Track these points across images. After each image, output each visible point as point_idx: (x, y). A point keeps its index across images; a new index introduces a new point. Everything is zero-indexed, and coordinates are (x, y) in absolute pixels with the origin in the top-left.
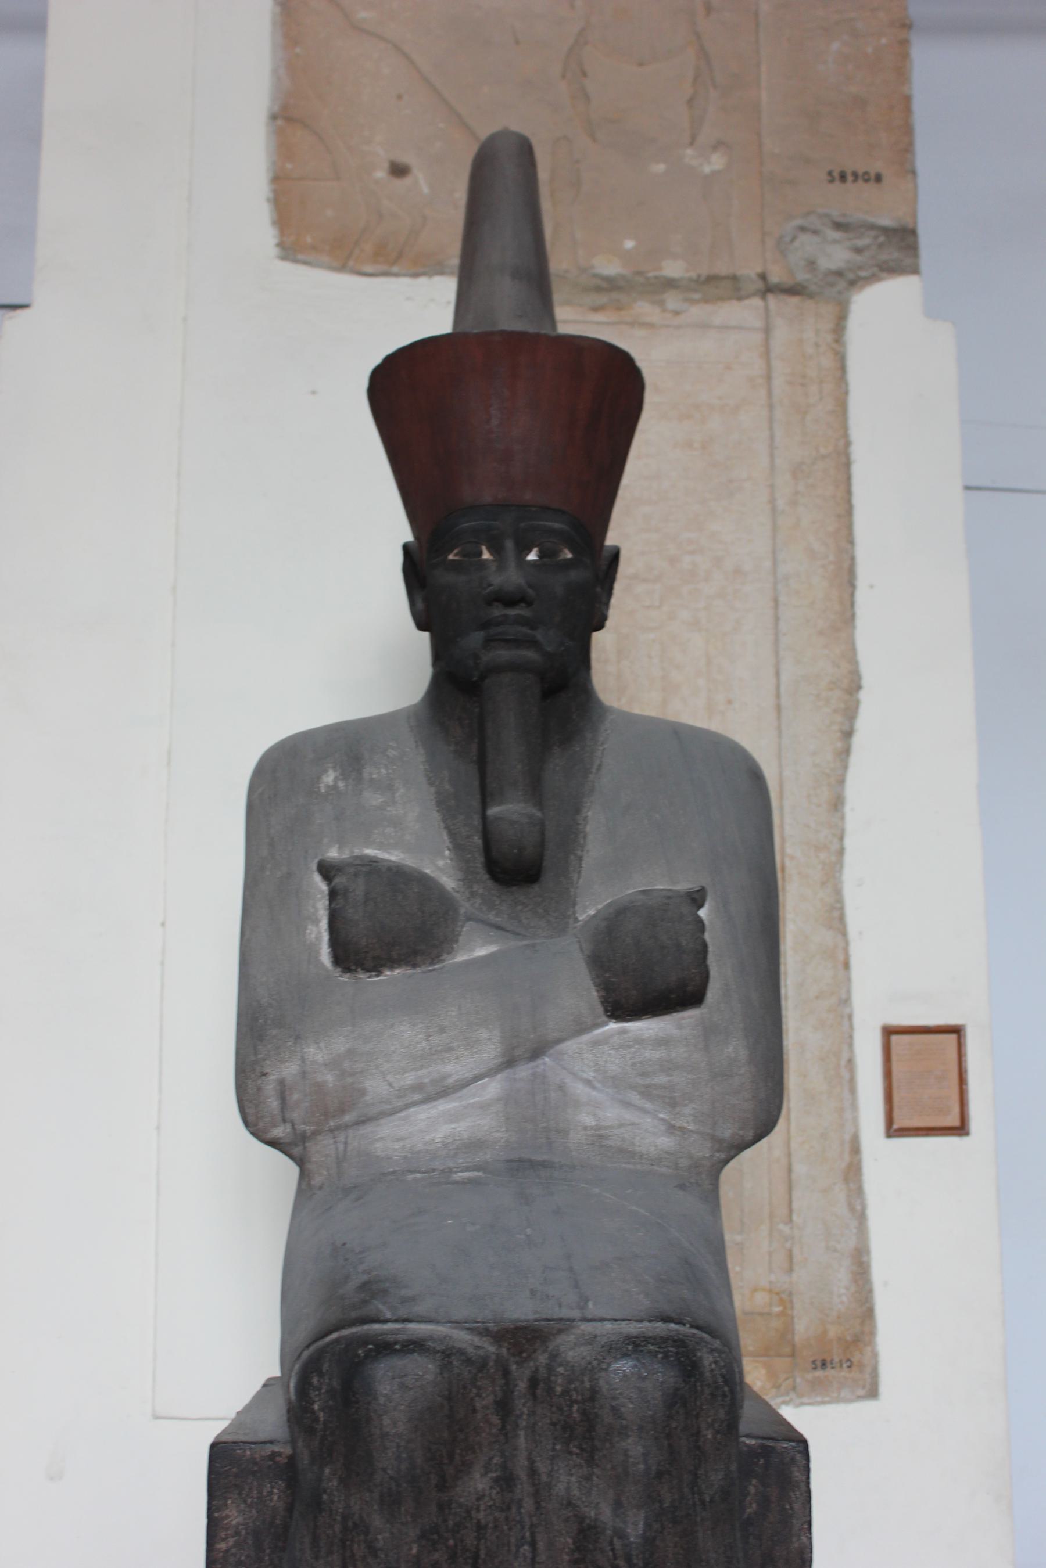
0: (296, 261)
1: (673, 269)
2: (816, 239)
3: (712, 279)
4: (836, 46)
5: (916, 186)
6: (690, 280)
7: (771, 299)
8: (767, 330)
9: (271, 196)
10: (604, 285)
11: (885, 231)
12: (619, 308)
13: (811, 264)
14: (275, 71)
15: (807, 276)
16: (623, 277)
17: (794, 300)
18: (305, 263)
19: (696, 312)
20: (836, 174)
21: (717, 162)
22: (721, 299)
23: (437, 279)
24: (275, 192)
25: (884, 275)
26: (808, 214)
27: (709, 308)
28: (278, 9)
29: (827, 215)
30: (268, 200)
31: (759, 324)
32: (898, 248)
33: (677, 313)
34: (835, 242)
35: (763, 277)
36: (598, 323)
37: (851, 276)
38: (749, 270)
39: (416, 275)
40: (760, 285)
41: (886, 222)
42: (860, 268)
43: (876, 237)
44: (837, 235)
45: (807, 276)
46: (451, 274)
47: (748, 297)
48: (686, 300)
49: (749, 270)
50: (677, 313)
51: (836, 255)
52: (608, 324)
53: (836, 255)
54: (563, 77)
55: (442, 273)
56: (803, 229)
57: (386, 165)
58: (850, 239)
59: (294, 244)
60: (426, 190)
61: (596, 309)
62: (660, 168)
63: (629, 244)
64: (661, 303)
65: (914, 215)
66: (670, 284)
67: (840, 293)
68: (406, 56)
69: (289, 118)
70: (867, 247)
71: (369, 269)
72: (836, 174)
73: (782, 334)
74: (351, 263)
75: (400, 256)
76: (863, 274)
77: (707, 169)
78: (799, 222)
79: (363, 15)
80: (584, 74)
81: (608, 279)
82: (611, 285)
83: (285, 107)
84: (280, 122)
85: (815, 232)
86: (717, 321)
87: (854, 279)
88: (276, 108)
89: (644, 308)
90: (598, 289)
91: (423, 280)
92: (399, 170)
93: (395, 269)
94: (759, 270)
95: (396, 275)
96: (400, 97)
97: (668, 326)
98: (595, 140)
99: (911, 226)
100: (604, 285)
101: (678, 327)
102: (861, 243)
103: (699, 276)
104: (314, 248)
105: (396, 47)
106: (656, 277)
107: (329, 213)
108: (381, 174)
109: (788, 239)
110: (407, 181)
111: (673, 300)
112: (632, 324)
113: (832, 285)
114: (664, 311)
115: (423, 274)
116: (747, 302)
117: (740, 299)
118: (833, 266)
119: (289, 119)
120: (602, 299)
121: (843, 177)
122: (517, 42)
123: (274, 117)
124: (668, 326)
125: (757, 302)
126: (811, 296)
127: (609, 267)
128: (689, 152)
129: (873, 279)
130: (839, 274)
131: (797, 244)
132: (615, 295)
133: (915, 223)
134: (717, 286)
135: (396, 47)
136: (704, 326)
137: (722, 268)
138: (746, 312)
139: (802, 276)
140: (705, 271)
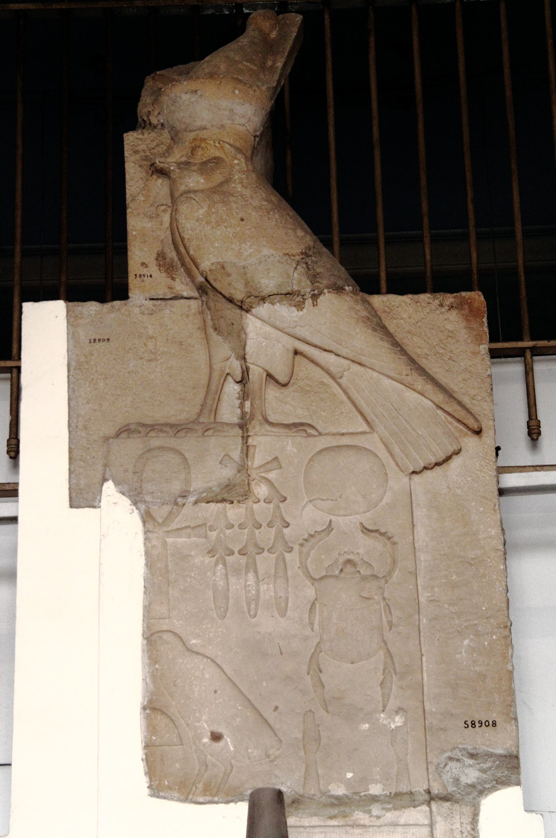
0: (158, 797)
1: (375, 789)
2: (458, 765)
3: (398, 795)
4: (466, 642)
5: (517, 726)
6: (386, 795)
7: (434, 805)
8: (431, 825)
9: (144, 757)
10: (336, 802)
11: (501, 756)
12: (345, 817)
13: (457, 781)
14: (144, 680)
15: (455, 789)
16: (346, 795)
17: (448, 804)
18: (165, 798)
19: (390, 816)
20: (469, 723)
21: (398, 721)
22: (405, 807)
23: (240, 804)
24: (146, 754)
25: (499, 786)
26: (454, 748)
27: (397, 813)
28: (145, 642)
29: (464, 749)
30: (143, 760)
31: (427, 822)
32: (508, 768)
33: (378, 817)
34: (470, 766)
35: (429, 792)
36: (333, 826)
37: (480, 788)
38: (420, 788)
39: (227, 802)
40: (427, 797)
41: (500, 751)
42: (485, 782)
43: (494, 762)
44: (471, 762)
45: (455, 789)
46: (247, 800)
47: (419, 805)
48: (383, 809)
49: (420, 788)
50: (378, 817)
51: (471, 775)
52: (338, 826)
53: (471, 775)
54: (308, 674)
55: (243, 800)
56: (451, 759)
57: (209, 734)
58: (478, 764)
59: (157, 789)
60: (232, 749)
61: (331, 818)
62: (367, 725)
63: (349, 775)
64: (369, 812)
65: (518, 747)
66: (374, 799)
67: (474, 798)
68: (218, 665)
69: (153, 708)
70: (490, 768)
71: (201, 799)
72: (469, 723)
73: (441, 826)
74: (191, 797)
75: (218, 791)
76: (487, 786)
77: (393, 726)
78: (448, 754)
79: (194, 641)
80: (321, 672)
81: (337, 798)
82: (339, 802)
83: (150, 701)
84: (148, 711)
85: (458, 760)
86: (402, 821)
87: (481, 790)
88: (145, 703)
89: (360, 816)
90: (332, 805)
91: (232, 805)
92: (216, 737)
93: (216, 799)
94: (425, 787)
95: (216, 803)
96: (215, 692)
97: (373, 826)
98: (327, 712)
99: (515, 753)
100: (336, 802)
101: (379, 827)
102: (485, 766)
103: (390, 793)
104: (169, 788)
105: (212, 660)
106: (365, 796)
107: (177, 765)
108: (206, 740)
109: (442, 766)
110: (221, 744)
111: (376, 810)
112: (353, 826)
113: (468, 794)
114: (371, 816)
115: (232, 801)
116: (419, 808)
117: (415, 807)
118: (469, 782)
119: (154, 709)
120: (335, 811)
121: (473, 724)
122: (282, 654)
123: (144, 708)
124: (373, 826)
125: (425, 808)
126: (457, 802)
127: (339, 790)
128: (382, 715)
129: (494, 789)
130: (473, 786)
131: (447, 768)
132: (342, 808)
133: (518, 751)
134: (401, 799)
135: (212, 660)
136: (395, 825)
137: (404, 788)
138: (418, 815)
139: (451, 789)
140: (393, 791)
